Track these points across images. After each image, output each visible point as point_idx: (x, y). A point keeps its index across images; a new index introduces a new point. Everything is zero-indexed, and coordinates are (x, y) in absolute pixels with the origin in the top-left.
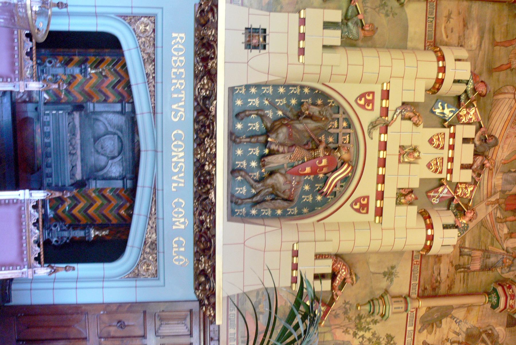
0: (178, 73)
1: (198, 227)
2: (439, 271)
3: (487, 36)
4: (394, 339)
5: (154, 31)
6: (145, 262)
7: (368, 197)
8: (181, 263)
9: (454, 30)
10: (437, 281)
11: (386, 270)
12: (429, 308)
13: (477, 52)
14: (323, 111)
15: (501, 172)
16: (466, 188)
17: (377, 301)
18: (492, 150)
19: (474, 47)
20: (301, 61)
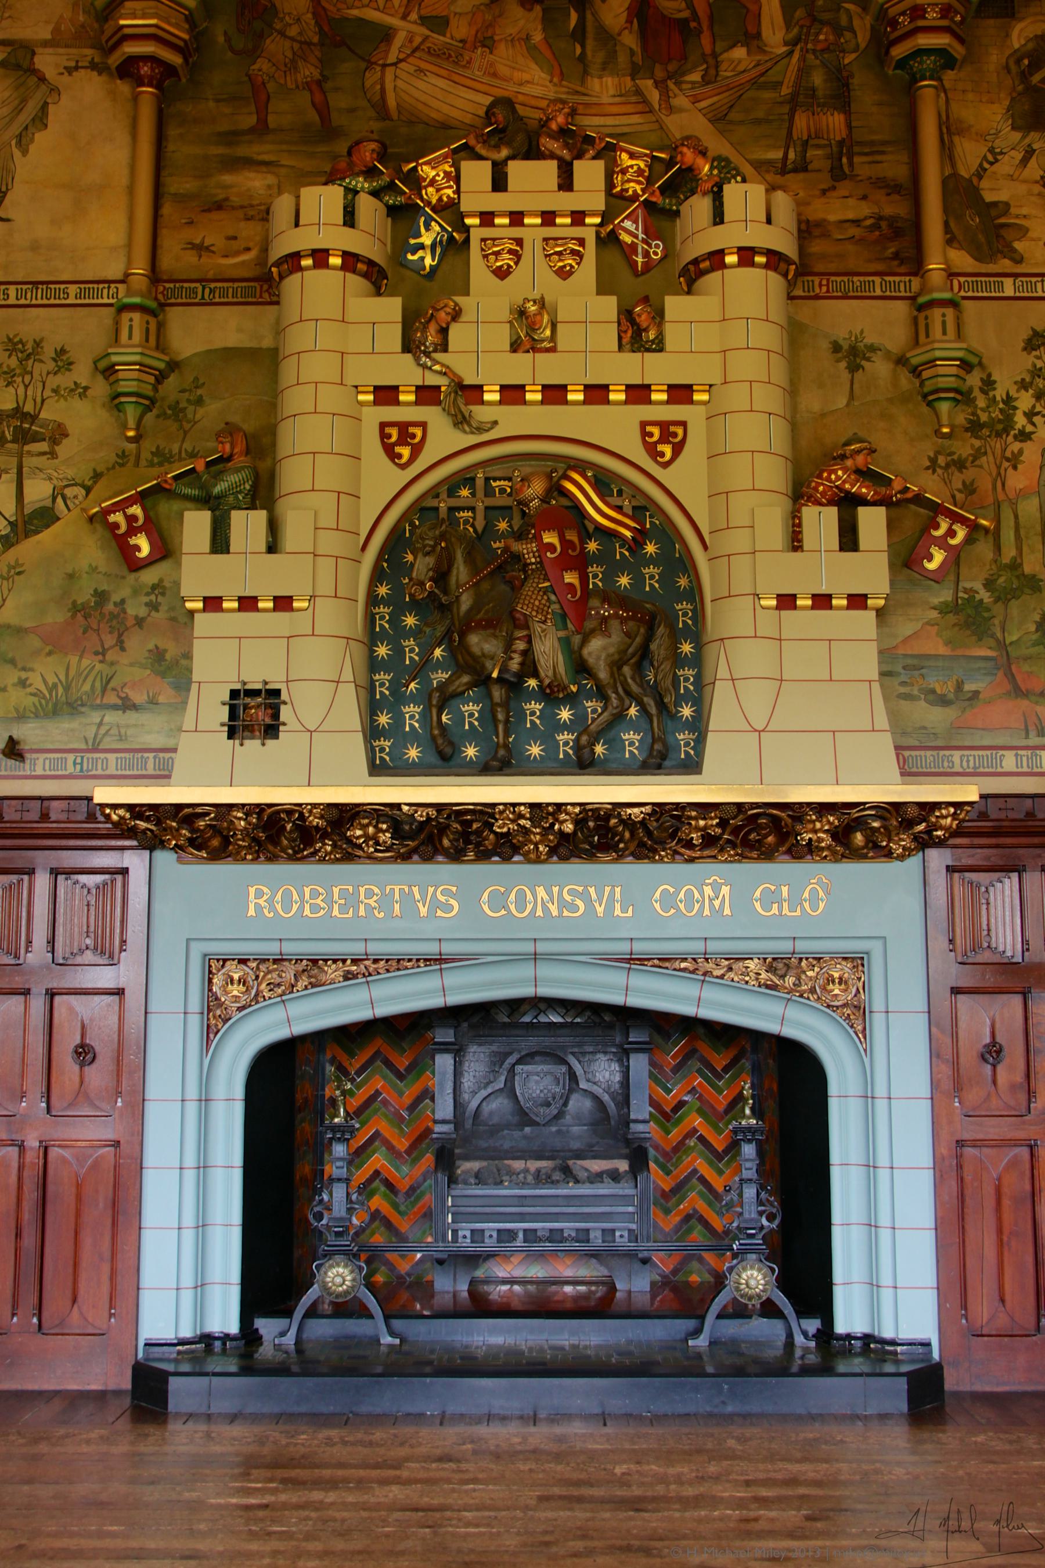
0: (343, 902)
1: (722, 850)
2: (848, 224)
3: (242, 151)
4: (1038, 329)
5: (243, 961)
6: (824, 989)
7: (644, 424)
8: (821, 893)
9: (231, 233)
10: (875, 227)
11: (843, 365)
12: (951, 241)
13: (283, 171)
14: (425, 546)
15: (583, 82)
16: (624, 171)
17: (927, 383)
18: (521, 110)
19: (271, 180)
20: (305, 604)
